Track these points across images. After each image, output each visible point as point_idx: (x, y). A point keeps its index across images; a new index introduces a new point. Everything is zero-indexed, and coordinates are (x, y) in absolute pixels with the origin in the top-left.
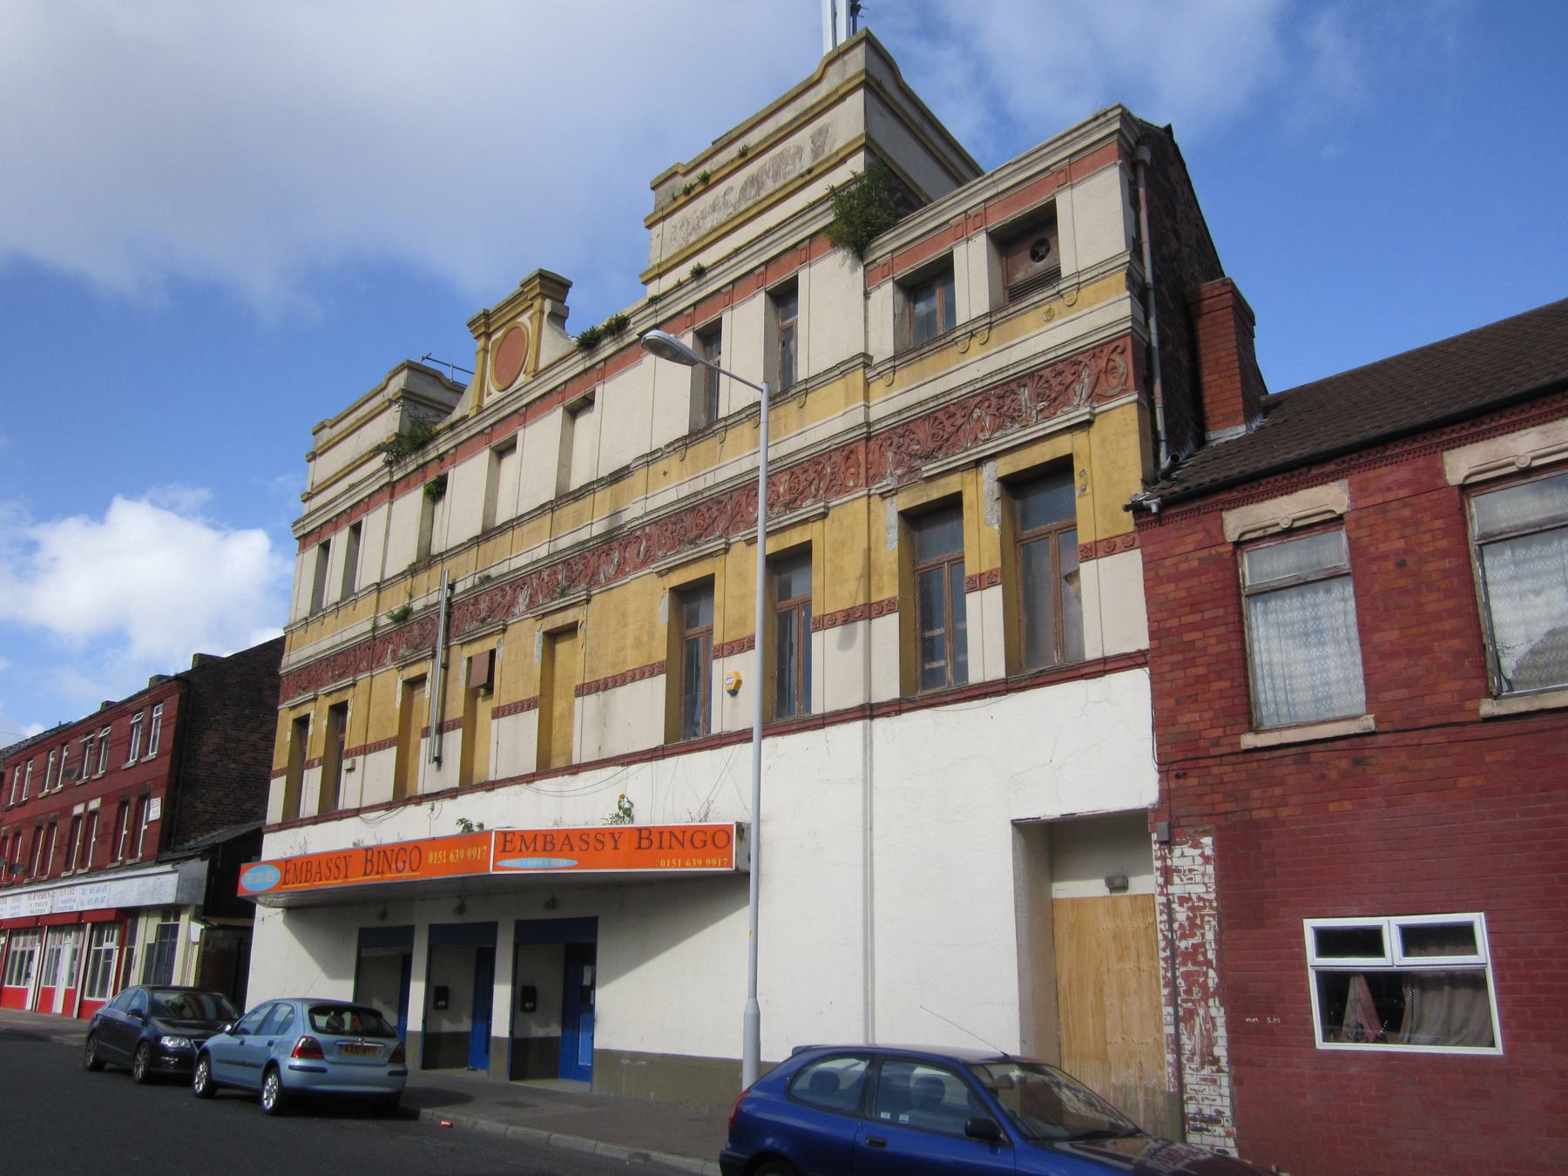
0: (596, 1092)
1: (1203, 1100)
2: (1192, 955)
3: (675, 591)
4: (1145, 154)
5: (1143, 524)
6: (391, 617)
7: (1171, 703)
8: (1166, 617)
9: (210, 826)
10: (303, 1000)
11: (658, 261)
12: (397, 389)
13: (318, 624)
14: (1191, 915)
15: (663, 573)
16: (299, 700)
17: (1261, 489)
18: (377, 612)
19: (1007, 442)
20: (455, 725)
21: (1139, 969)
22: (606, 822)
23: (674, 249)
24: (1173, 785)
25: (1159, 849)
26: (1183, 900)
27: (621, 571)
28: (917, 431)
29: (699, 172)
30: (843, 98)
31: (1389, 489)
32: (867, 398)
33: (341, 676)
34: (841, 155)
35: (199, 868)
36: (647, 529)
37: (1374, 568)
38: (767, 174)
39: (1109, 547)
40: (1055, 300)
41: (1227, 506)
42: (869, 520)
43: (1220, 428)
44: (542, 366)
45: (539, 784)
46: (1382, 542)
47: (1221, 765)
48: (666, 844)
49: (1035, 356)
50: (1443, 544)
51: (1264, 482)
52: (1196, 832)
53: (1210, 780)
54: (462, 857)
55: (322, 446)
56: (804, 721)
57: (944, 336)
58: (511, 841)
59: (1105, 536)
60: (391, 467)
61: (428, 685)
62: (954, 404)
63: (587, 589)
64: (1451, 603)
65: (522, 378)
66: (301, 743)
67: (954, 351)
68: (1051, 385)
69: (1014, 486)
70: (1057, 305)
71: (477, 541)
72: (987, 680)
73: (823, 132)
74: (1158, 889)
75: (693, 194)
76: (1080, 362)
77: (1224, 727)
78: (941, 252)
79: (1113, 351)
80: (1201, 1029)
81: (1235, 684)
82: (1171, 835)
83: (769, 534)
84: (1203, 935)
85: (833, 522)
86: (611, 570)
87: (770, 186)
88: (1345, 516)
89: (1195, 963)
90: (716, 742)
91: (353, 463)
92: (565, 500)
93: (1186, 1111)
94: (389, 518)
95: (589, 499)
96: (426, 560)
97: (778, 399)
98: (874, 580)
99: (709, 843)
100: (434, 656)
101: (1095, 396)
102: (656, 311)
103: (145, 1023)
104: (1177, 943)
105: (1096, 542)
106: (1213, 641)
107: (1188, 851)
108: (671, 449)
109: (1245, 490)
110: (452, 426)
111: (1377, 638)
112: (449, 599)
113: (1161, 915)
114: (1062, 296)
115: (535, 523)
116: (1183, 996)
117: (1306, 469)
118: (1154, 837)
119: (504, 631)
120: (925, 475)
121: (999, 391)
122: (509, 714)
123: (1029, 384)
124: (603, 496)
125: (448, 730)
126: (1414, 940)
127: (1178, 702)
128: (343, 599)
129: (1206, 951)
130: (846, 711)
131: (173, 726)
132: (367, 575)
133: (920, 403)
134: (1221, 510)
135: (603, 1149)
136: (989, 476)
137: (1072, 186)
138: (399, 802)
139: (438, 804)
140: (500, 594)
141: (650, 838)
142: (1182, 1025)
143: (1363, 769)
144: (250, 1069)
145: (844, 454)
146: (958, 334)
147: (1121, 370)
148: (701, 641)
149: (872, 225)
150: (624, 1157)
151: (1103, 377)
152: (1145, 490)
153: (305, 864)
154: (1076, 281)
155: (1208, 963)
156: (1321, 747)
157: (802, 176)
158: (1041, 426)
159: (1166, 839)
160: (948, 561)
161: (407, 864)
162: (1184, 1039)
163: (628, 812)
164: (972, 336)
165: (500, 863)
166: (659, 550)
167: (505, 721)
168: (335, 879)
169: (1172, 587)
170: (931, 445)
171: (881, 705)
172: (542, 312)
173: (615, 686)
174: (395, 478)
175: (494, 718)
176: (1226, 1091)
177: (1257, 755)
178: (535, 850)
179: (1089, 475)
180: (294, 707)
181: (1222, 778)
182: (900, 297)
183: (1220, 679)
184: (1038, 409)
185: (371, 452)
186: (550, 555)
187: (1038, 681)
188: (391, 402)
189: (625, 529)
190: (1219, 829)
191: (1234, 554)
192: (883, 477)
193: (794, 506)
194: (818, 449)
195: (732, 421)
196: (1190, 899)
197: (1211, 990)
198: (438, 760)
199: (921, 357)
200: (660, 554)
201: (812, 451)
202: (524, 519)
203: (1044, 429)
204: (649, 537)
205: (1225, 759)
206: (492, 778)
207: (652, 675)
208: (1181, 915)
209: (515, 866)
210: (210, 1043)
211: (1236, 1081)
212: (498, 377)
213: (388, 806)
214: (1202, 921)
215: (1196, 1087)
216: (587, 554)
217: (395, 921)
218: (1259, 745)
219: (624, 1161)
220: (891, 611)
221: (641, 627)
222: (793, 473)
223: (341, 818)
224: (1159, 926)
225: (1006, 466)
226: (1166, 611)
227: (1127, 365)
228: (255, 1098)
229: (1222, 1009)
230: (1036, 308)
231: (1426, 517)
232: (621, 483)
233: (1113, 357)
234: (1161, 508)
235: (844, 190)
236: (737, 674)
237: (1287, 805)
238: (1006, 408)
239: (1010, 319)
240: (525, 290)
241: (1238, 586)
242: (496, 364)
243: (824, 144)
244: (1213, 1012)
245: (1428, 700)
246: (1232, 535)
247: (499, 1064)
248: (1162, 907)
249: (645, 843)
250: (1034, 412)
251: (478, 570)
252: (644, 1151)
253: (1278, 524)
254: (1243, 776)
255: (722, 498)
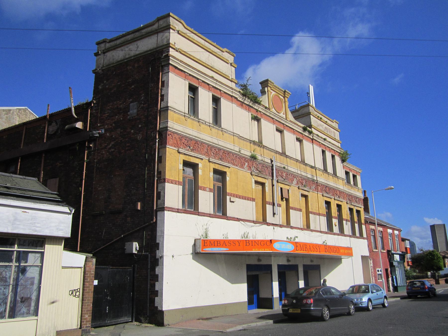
139: (276, 228)
161: (336, 251)
202: (292, 159)
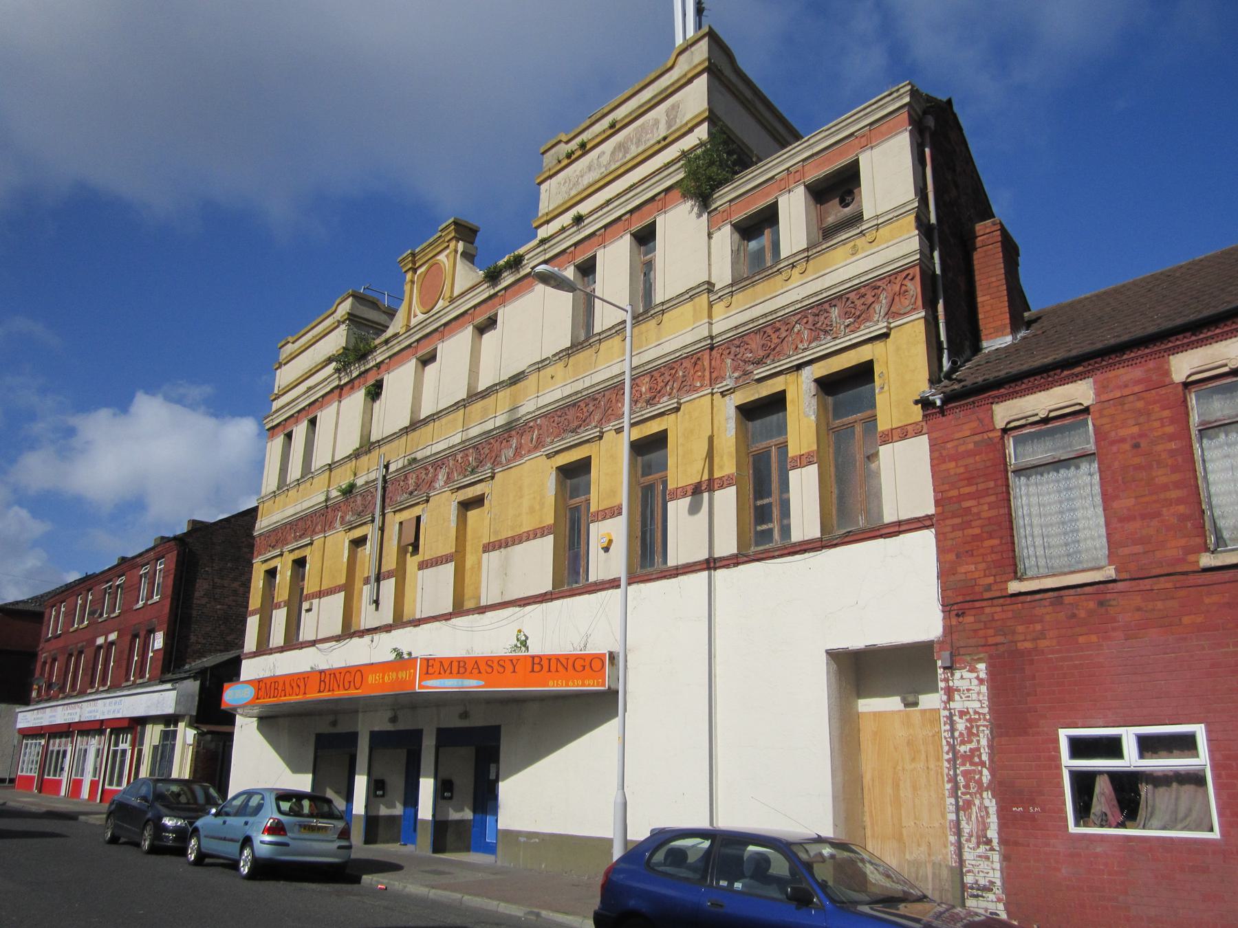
0: (499, 863)
1: (979, 873)
2: (969, 757)
3: (561, 469)
4: (930, 122)
5: (929, 415)
6: (340, 491)
7: (951, 557)
8: (947, 488)
9: (201, 654)
10: (271, 790)
11: (547, 211)
12: (344, 313)
13: (283, 496)
14: (969, 725)
15: (551, 455)
16: (269, 555)
17: (1024, 386)
18: (329, 487)
19: (820, 351)
20: (389, 575)
21: (928, 768)
22: (506, 651)
23: (560, 201)
24: (954, 621)
25: (944, 673)
26: (962, 714)
27: (518, 454)
28: (750, 342)
29: (578, 140)
30: (690, 81)
31: (1126, 386)
32: (710, 316)
33: (301, 537)
34: (690, 125)
35: (193, 686)
36: (539, 421)
37: (1114, 448)
38: (632, 141)
39: (903, 433)
40: (858, 238)
41: (996, 400)
42: (712, 413)
43: (992, 338)
44: (456, 294)
45: (454, 621)
46: (1121, 428)
47: (992, 606)
48: (553, 668)
49: (843, 282)
50: (1170, 429)
51: (1026, 381)
52: (973, 659)
53: (983, 618)
54: (394, 677)
55: (286, 357)
56: (662, 572)
57: (771, 267)
58: (433, 666)
59: (900, 425)
60: (340, 374)
61: (368, 543)
62: (779, 321)
63: (491, 468)
64: (1176, 477)
65: (441, 304)
66: (270, 589)
67: (779, 278)
68: (856, 305)
69: (827, 385)
70: (860, 242)
71: (406, 431)
72: (806, 539)
73: (675, 107)
74: (943, 705)
75: (573, 157)
76: (879, 287)
77: (994, 576)
78: (769, 200)
79: (905, 278)
80: (977, 817)
81: (1003, 541)
82: (952, 662)
83: (633, 425)
84: (978, 741)
85: (684, 414)
86: (511, 453)
87: (634, 150)
88: (1091, 407)
89: (972, 764)
90: (593, 588)
91: (311, 370)
92: (474, 398)
93: (965, 881)
94: (338, 413)
95: (493, 397)
96: (367, 447)
97: (641, 318)
98: (716, 460)
99: (588, 667)
100: (373, 521)
101: (891, 314)
102: (545, 250)
103: (151, 806)
104: (958, 747)
105: (892, 430)
106: (986, 507)
107: (967, 674)
108: (557, 358)
109: (1010, 387)
110: (387, 342)
111: (1115, 505)
112: (384, 477)
113: (945, 725)
114: (864, 235)
115: (451, 417)
116: (963, 790)
117: (1059, 371)
118: (939, 663)
119: (427, 501)
120: (757, 377)
121: (814, 310)
122: (432, 566)
123: (839, 304)
124: (504, 395)
125: (384, 579)
126: (1148, 745)
127: (958, 556)
128: (302, 477)
129: (981, 754)
130: (695, 564)
131: (172, 576)
132: (321, 457)
133: (752, 321)
134: (992, 403)
135: (505, 908)
136: (807, 377)
137: (872, 148)
138: (345, 635)
139: (376, 637)
140: (424, 472)
141: (540, 664)
142: (962, 813)
143: (1107, 610)
144: (230, 843)
145: (693, 361)
146: (782, 265)
147: (912, 292)
148: (583, 508)
149: (714, 181)
150: (520, 914)
151: (897, 298)
152: (931, 388)
153: (273, 685)
154: (875, 222)
155: (983, 764)
156: (1072, 592)
157: (659, 142)
158: (848, 338)
159: (949, 665)
160: (775, 445)
161: (352, 684)
162: (963, 824)
163: (524, 644)
164: (793, 266)
165: (424, 683)
166: (548, 437)
167: (428, 572)
168: (297, 695)
169: (953, 464)
170: (761, 353)
171: (721, 559)
172: (456, 251)
173: (513, 544)
174: (342, 383)
175: (419, 569)
176: (997, 866)
177: (1021, 598)
178: (451, 673)
179: (886, 375)
180: (265, 561)
181: (993, 617)
182: (737, 236)
183: (991, 537)
184: (846, 324)
185: (324, 361)
186: (463, 442)
187: (846, 540)
188: (339, 323)
189: (522, 421)
190: (991, 657)
191: (1002, 438)
192: (724, 379)
193: (653, 402)
194: (673, 357)
195: (604, 335)
196: (968, 712)
197: (985, 785)
198: (377, 602)
199: (753, 284)
200: (549, 440)
201: (668, 359)
203: (850, 340)
204: (540, 427)
205: (995, 602)
206: (418, 616)
207: (543, 536)
208: (961, 725)
209: (435, 685)
210: (199, 823)
211: (1006, 858)
212: (422, 302)
213: (338, 639)
214: (978, 730)
215: (973, 862)
216: (492, 441)
217: (341, 729)
218: (1023, 590)
219: (520, 918)
220: (730, 485)
221: (534, 498)
222: (652, 376)
223: (302, 648)
224: (943, 735)
225: (821, 370)
226: (948, 484)
227: (916, 289)
228: (234, 865)
229: (994, 801)
230: (844, 244)
231: (1157, 408)
232: (518, 385)
233: (904, 282)
234: (944, 402)
235: (691, 153)
236: (609, 534)
237: (1045, 638)
238: (820, 324)
239: (823, 254)
240: (443, 234)
241: (1006, 464)
242: (420, 292)
243: (676, 117)
244: (987, 803)
245: (1158, 554)
246: (1000, 424)
247: (425, 839)
248: (945, 719)
249: (537, 668)
250: (842, 327)
251: (407, 454)
252: (536, 910)
253: (1037, 415)
254: (1010, 614)
255: (597, 396)
